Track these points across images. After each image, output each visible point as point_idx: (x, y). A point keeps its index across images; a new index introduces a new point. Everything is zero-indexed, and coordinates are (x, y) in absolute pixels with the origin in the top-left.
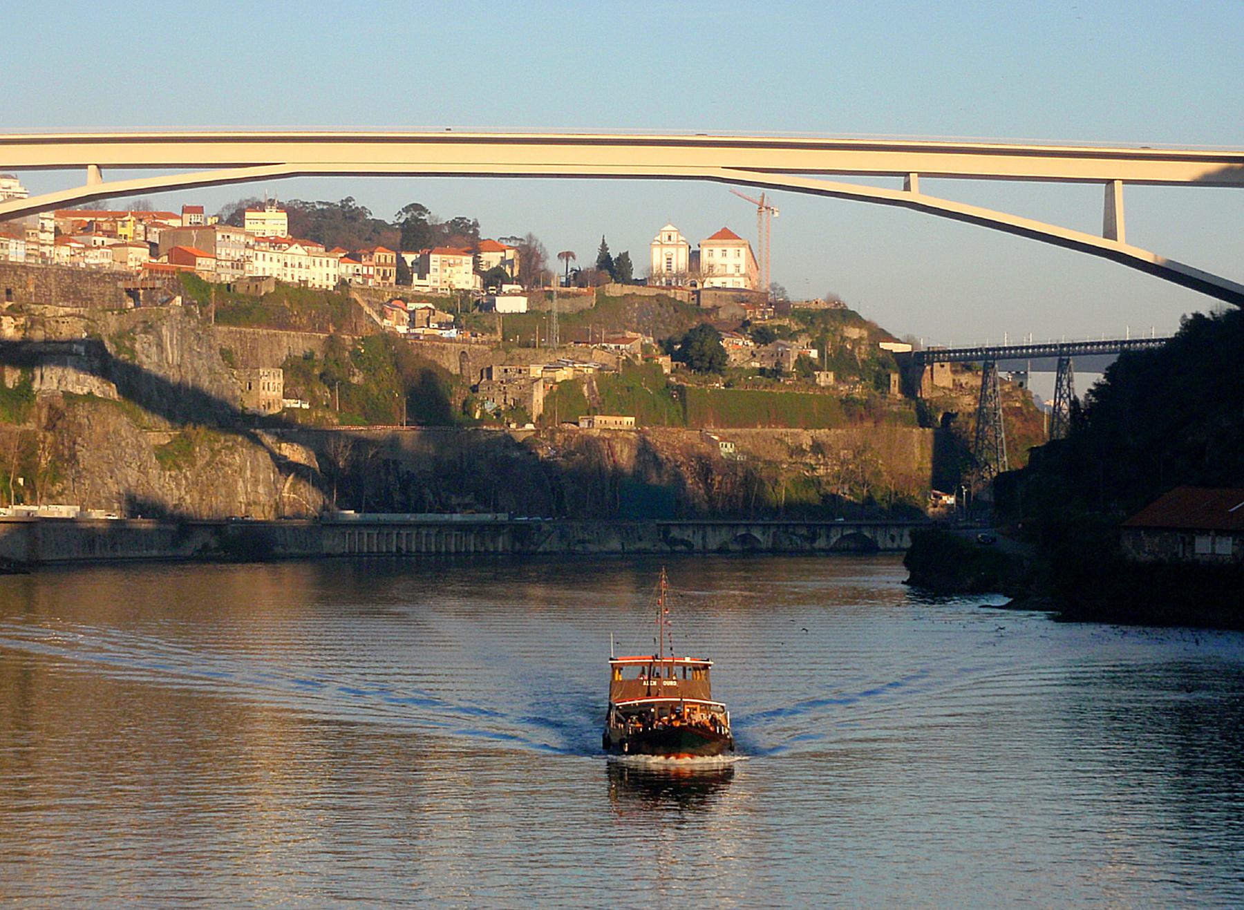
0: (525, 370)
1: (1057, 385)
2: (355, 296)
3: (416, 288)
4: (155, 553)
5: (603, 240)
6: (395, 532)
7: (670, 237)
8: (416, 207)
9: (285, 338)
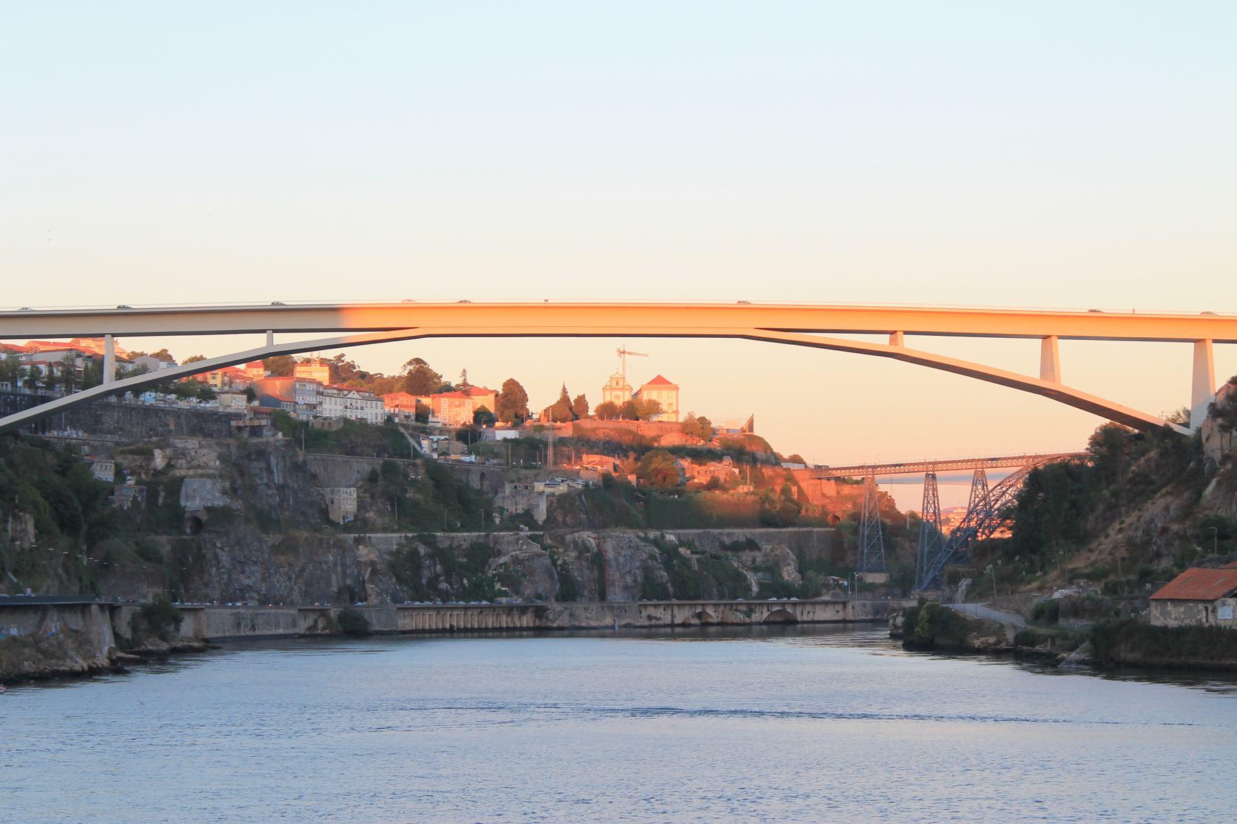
0: (531, 486)
1: (925, 494)
2: (402, 430)
3: (431, 424)
4: (281, 631)
5: (564, 388)
6: (449, 613)
7: (617, 383)
8: (418, 361)
9: (355, 464)
